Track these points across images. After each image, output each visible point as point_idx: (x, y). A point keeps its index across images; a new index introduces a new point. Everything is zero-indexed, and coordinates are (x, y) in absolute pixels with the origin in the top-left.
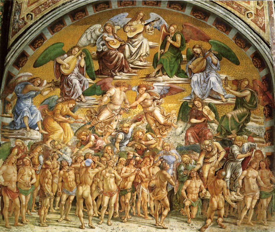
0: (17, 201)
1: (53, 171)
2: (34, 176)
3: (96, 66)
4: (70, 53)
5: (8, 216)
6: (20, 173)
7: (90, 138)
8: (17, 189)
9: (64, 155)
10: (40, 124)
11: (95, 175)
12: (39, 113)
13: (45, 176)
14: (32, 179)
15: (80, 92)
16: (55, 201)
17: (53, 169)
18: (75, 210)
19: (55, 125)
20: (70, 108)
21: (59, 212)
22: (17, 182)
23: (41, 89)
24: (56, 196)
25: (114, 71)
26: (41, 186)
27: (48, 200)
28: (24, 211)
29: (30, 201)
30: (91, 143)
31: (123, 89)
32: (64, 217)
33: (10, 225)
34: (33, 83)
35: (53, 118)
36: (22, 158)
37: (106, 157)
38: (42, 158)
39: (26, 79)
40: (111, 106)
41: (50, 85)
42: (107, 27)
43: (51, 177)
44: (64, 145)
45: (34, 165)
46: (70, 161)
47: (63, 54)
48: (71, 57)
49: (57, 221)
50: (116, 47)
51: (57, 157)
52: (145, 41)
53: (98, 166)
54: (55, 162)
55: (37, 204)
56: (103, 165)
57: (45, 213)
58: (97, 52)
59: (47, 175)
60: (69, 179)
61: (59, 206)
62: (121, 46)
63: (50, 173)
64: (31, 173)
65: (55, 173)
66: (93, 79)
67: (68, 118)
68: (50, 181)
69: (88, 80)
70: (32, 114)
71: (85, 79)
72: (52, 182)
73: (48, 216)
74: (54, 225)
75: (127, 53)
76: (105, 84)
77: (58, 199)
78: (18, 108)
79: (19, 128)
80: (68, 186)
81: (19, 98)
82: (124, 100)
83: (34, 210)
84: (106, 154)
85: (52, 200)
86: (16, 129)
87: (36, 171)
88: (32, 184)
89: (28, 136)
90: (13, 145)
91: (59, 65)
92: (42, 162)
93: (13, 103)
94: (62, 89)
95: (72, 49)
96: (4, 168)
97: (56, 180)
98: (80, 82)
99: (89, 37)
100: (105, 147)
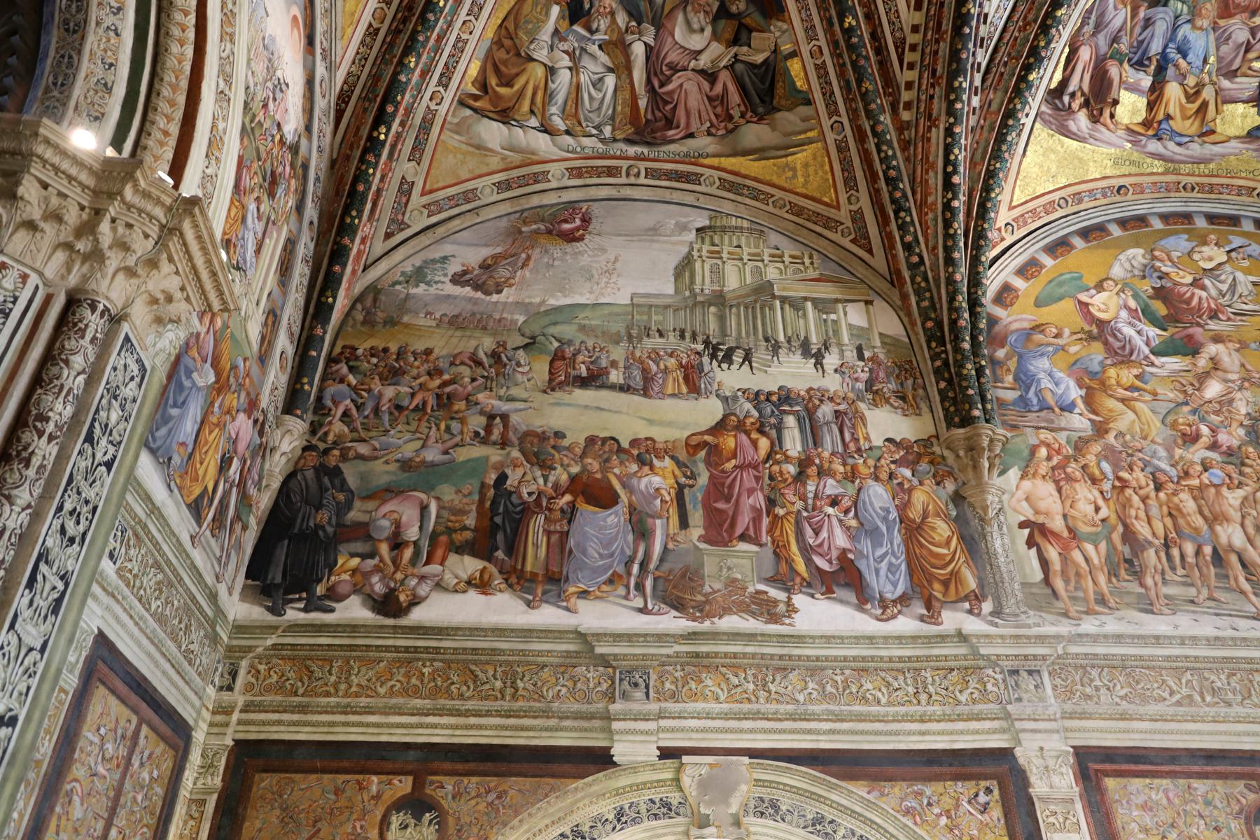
0: (1077, 556)
1: (1142, 492)
2: (1101, 502)
3: (1160, 309)
4: (1100, 287)
5: (1067, 590)
6: (1067, 497)
7: (1198, 430)
8: (1070, 530)
9: (1155, 462)
10: (1080, 403)
11: (1242, 503)
12: (1072, 383)
13: (1126, 504)
14: (1097, 509)
15: (1146, 350)
16: (1169, 557)
17: (1141, 488)
18: (1227, 577)
19: (1112, 404)
20: (1136, 377)
21: (1189, 580)
22: (1065, 516)
23: (1060, 341)
24: (1167, 546)
25: (1200, 317)
26: (1126, 526)
27: (1152, 552)
28: (1102, 579)
29: (1108, 557)
30: (1205, 440)
31: (1230, 345)
32: (1205, 592)
33: (1077, 611)
34: (1042, 332)
35: (1105, 391)
36: (1062, 466)
37: (1251, 466)
38: (1106, 466)
39: (1026, 325)
40: (1219, 373)
41: (1079, 336)
42: (1157, 253)
43: (1142, 506)
44: (1147, 442)
45: (1094, 481)
46: (1173, 473)
47: (1088, 290)
48: (1104, 295)
49: (1192, 602)
50: (1189, 279)
51: (1140, 464)
52: (1240, 276)
53: (1240, 483)
54: (1138, 473)
55: (1129, 562)
56: (1250, 483)
57: (1156, 584)
58: (1153, 288)
59: (1129, 500)
60: (1185, 511)
61: (1184, 568)
62: (1195, 280)
63: (1136, 499)
64: (1090, 496)
65: (1147, 497)
66: (1165, 330)
67: (1136, 394)
68: (1142, 514)
69: (1153, 332)
70: (1057, 384)
71: (1146, 328)
72: (1147, 516)
73: (1166, 590)
74: (1188, 611)
75: (1214, 293)
76: (1190, 337)
77: (1175, 552)
78: (1025, 375)
79: (1036, 408)
80: (1189, 524)
81: (1020, 356)
82: (1243, 365)
83: (1127, 577)
84: (1247, 461)
85: (1163, 555)
86: (1030, 411)
87: (1102, 493)
88: (1103, 521)
89: (1063, 425)
90: (1033, 441)
91: (1084, 306)
92: (1111, 476)
93: (1012, 364)
94: (1106, 343)
95: (1102, 282)
96: (1027, 484)
97: (1154, 511)
98: (1139, 332)
99: (1127, 266)
100: (1239, 447)
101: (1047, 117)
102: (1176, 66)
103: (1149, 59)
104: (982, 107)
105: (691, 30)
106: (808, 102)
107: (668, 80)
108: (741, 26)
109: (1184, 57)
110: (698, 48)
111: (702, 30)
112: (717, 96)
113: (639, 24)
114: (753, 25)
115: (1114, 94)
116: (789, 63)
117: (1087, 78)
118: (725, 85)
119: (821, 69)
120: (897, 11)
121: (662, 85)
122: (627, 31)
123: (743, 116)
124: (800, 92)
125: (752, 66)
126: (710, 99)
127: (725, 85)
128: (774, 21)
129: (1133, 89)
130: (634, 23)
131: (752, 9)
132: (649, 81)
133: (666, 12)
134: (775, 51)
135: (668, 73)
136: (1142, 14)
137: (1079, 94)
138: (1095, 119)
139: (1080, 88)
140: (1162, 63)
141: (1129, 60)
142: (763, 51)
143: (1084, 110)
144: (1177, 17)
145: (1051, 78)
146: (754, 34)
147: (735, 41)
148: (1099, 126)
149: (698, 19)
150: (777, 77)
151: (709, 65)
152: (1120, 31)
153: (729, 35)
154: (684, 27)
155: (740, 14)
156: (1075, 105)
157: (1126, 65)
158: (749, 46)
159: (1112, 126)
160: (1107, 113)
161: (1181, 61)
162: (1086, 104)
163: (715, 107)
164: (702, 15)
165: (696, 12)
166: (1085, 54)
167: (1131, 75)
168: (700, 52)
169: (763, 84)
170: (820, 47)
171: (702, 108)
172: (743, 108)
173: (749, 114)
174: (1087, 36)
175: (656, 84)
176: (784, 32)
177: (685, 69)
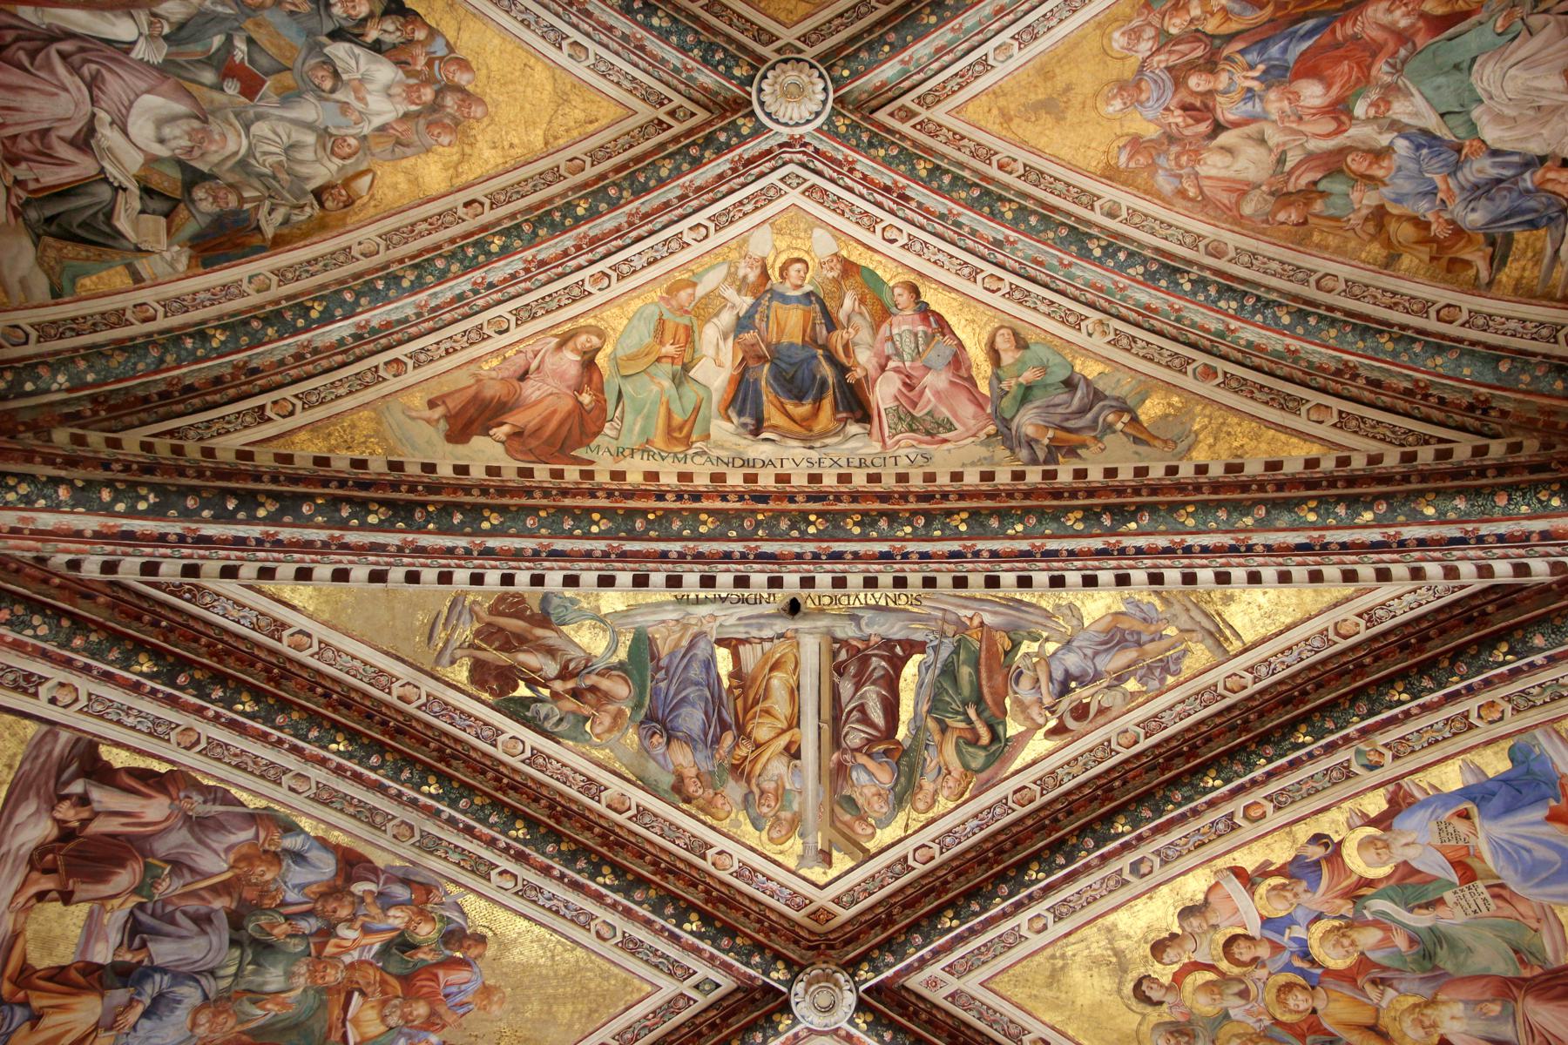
101: (46, 748)
102: (130, 1005)
103: (144, 945)
104: (81, 582)
105: (161, 122)
106: (57, 294)
107: (75, 70)
108: (176, 202)
109: (147, 1014)
110: (131, 130)
111: (162, 141)
112: (50, 148)
113: (166, 38)
114: (177, 221)
115: (83, 890)
116: (120, 269)
117: (113, 826)
118: (70, 163)
119: (118, 318)
120: (228, 432)
121: (64, 56)
122: (154, 15)
123: (18, 183)
124: (74, 283)
125: (109, 214)
126: (44, 133)
127: (70, 163)
128: (187, 252)
129: (92, 929)
130: (166, 30)
131: (204, 221)
132: (69, 35)
133: (187, 85)
134: (139, 250)
135: (85, 70)
136: (219, 903)
137: (85, 814)
138: (39, 860)
139: (96, 814)
140: (135, 974)
141: (141, 906)
142: (136, 232)
143: (55, 832)
144: (212, 972)
145: (117, 744)
146: (163, 221)
147: (147, 191)
148: (23, 870)
149: (179, 137)
150: (94, 250)
151: (105, 144)
152: (192, 870)
153: (156, 182)
154: (165, 112)
155: (193, 201)
156: (66, 811)
157: (134, 901)
158: (142, 212)
159: (21, 900)
160: (47, 883)
161: (140, 1009)
162: (67, 834)
163: (29, 138)
164: (185, 142)
165: (190, 134)
166: (155, 809)
167: (115, 917)
168: (125, 132)
169: (79, 226)
170: (153, 319)
171: (28, 117)
172: (32, 186)
173: (24, 195)
174: (185, 805)
175: (67, 46)
176: (171, 265)
177: (94, 101)
